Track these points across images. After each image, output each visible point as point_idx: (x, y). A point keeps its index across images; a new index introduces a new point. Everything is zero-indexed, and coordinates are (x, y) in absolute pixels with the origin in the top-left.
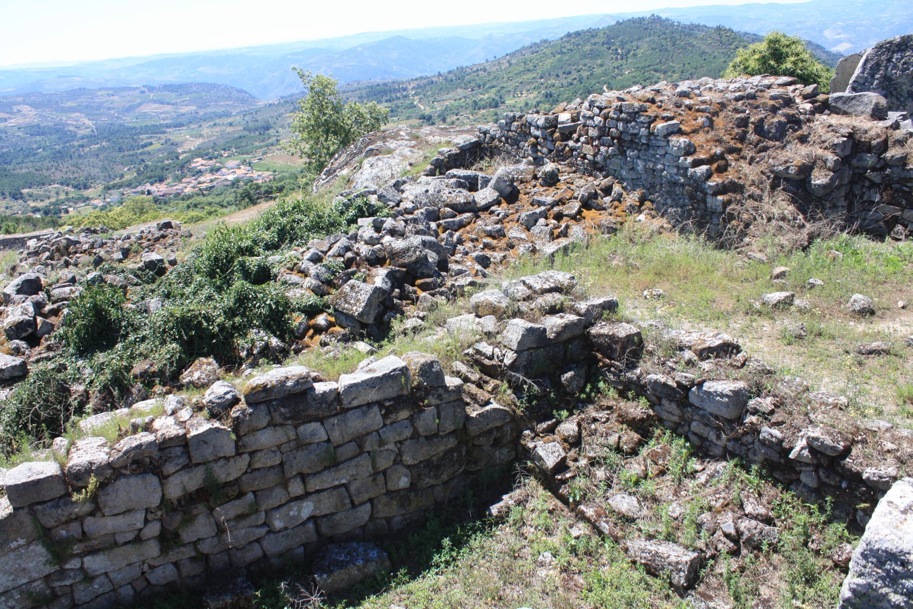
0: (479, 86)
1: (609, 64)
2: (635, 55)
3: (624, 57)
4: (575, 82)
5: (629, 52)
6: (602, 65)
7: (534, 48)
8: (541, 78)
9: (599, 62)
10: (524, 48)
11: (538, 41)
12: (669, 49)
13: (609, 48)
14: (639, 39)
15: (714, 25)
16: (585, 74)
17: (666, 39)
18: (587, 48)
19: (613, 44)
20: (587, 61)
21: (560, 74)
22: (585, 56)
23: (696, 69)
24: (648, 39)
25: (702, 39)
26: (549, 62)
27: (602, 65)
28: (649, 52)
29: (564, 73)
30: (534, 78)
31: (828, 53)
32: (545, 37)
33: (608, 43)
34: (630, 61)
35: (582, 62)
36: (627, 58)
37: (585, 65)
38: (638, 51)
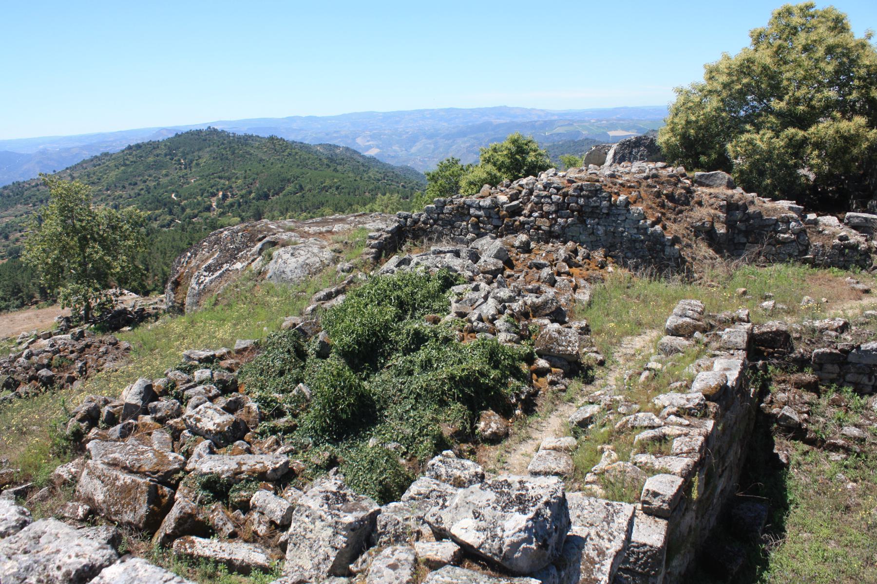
0: (41, 201)
1: (175, 174)
2: (198, 164)
3: (188, 166)
4: (142, 192)
5: (191, 161)
6: (167, 175)
7: (96, 161)
8: (108, 190)
9: (164, 172)
10: (84, 161)
11: (98, 154)
12: (230, 157)
13: (172, 159)
14: (199, 150)
15: (267, 135)
16: (152, 184)
17: (225, 148)
18: (151, 159)
19: (176, 155)
20: (152, 172)
21: (127, 186)
22: (149, 167)
23: (257, 174)
24: (208, 149)
25: (258, 148)
26: (113, 175)
27: (167, 175)
28: (211, 161)
29: (130, 184)
30: (100, 190)
31: (364, 157)
32: (106, 151)
33: (170, 154)
34: (193, 170)
35: (147, 173)
36: (190, 168)
37: (150, 176)
38: (200, 161)
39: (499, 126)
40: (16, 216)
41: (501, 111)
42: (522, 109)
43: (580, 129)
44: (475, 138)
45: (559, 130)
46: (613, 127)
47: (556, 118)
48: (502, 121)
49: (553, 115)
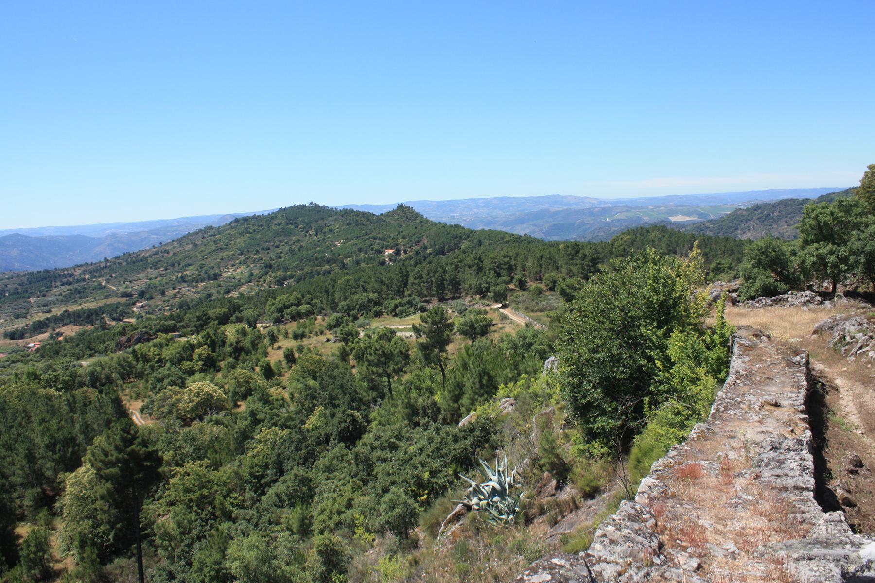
0: (173, 265)
39: (556, 213)
40: (150, 279)
41: (555, 199)
42: (575, 197)
43: (641, 215)
44: (534, 225)
45: (618, 216)
46: (675, 213)
47: (610, 205)
48: (557, 209)
49: (605, 203)
